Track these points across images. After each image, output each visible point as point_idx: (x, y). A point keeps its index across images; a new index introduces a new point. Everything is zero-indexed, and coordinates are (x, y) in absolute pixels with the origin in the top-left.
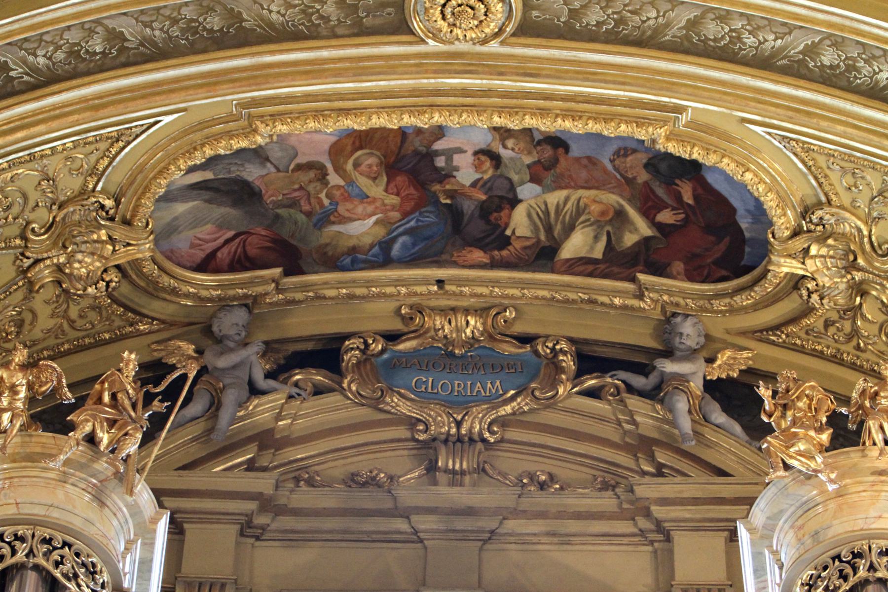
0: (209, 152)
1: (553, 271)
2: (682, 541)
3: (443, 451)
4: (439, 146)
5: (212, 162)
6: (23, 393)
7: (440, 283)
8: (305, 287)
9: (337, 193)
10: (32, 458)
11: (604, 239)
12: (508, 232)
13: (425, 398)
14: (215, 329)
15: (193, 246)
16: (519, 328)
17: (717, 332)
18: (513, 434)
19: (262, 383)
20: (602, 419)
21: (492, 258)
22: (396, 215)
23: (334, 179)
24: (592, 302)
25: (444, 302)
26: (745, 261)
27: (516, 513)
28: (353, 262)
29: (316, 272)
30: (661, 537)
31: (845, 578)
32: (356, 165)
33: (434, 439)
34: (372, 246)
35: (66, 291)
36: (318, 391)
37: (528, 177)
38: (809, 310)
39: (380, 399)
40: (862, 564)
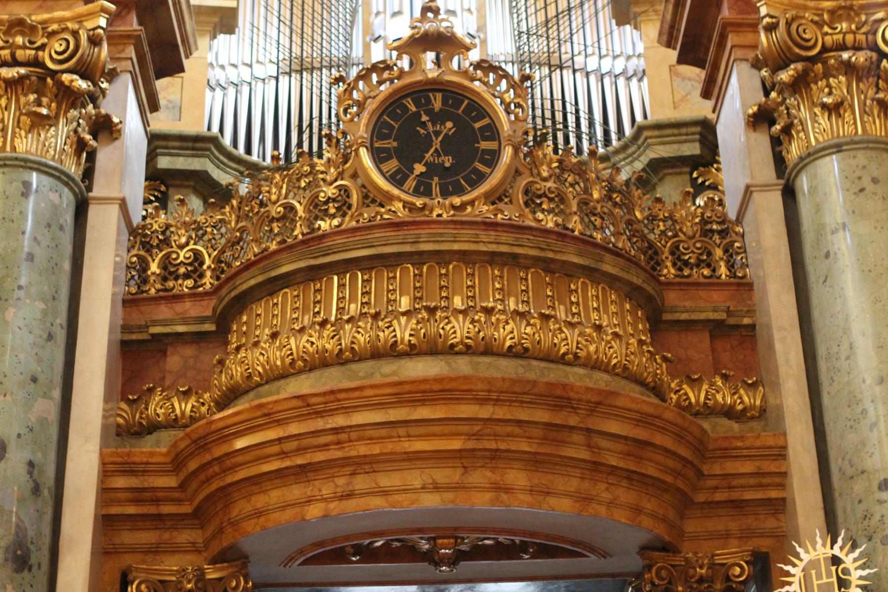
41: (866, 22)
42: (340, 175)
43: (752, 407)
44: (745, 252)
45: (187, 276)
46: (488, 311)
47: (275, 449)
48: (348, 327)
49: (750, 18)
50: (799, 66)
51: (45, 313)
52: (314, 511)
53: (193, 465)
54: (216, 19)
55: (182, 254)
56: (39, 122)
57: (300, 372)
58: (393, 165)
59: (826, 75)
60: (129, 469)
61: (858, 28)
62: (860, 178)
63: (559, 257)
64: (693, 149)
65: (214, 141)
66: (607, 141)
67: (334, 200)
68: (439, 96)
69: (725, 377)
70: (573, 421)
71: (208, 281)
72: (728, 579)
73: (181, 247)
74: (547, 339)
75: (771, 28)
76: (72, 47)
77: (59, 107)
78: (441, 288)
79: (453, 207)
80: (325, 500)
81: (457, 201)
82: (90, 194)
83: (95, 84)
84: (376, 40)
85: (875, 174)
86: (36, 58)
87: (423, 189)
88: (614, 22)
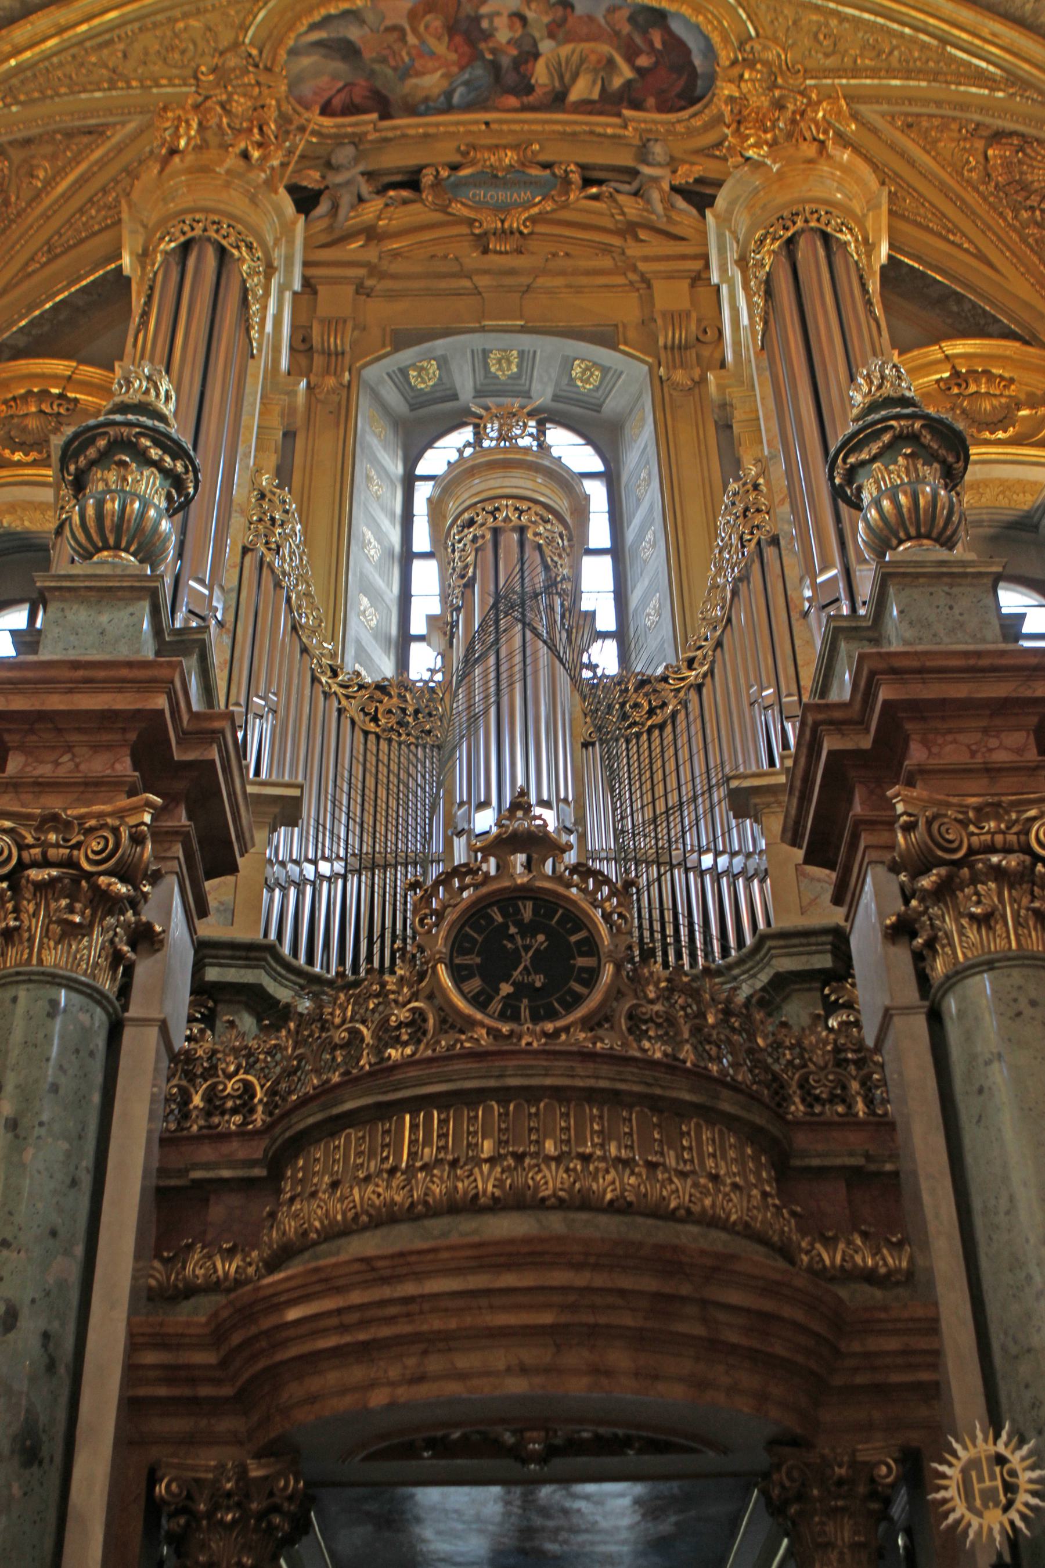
0: (323, 12)
1: (564, 111)
2: (658, 285)
3: (493, 239)
4: (484, 10)
5: (328, 19)
7: (487, 124)
8: (394, 128)
9: (414, 52)
11: (599, 83)
12: (533, 81)
13: (480, 206)
14: (333, 161)
15: (315, 93)
16: (543, 158)
17: (678, 154)
18: (541, 229)
20: (600, 214)
21: (522, 103)
22: (455, 69)
23: (412, 39)
24: (592, 133)
26: (698, 92)
27: (545, 272)
28: (428, 109)
29: (401, 117)
30: (644, 285)
31: (786, 228)
32: (427, 27)
33: (485, 234)
34: (439, 96)
36: (405, 202)
37: (546, 34)
41: (1017, 821)
42: (415, 996)
43: (898, 1270)
44: (886, 1085)
45: (235, 1111)
46: (586, 1158)
47: (334, 1321)
48: (420, 1176)
49: (884, 815)
50: (943, 871)
51: (68, 1155)
52: (378, 1398)
53: (236, 1339)
55: (230, 1086)
56: (71, 931)
57: (365, 1228)
58: (475, 984)
59: (974, 881)
60: (162, 1342)
61: (1008, 828)
62: (1015, 1000)
63: (669, 1093)
64: (825, 961)
65: (272, 950)
66: (725, 951)
67: (407, 1025)
68: (529, 904)
69: (865, 1235)
70: (685, 1290)
71: (259, 1117)
72: (872, 1480)
73: (230, 1077)
74: (654, 1191)
75: (908, 828)
76: (111, 846)
77: (94, 915)
78: (530, 1130)
79: (545, 1034)
80: (392, 1384)
81: (549, 1027)
82: (126, 1015)
83: (136, 888)
84: (459, 834)
85: (1033, 995)
86: (70, 856)
87: (510, 1013)
88: (731, 814)
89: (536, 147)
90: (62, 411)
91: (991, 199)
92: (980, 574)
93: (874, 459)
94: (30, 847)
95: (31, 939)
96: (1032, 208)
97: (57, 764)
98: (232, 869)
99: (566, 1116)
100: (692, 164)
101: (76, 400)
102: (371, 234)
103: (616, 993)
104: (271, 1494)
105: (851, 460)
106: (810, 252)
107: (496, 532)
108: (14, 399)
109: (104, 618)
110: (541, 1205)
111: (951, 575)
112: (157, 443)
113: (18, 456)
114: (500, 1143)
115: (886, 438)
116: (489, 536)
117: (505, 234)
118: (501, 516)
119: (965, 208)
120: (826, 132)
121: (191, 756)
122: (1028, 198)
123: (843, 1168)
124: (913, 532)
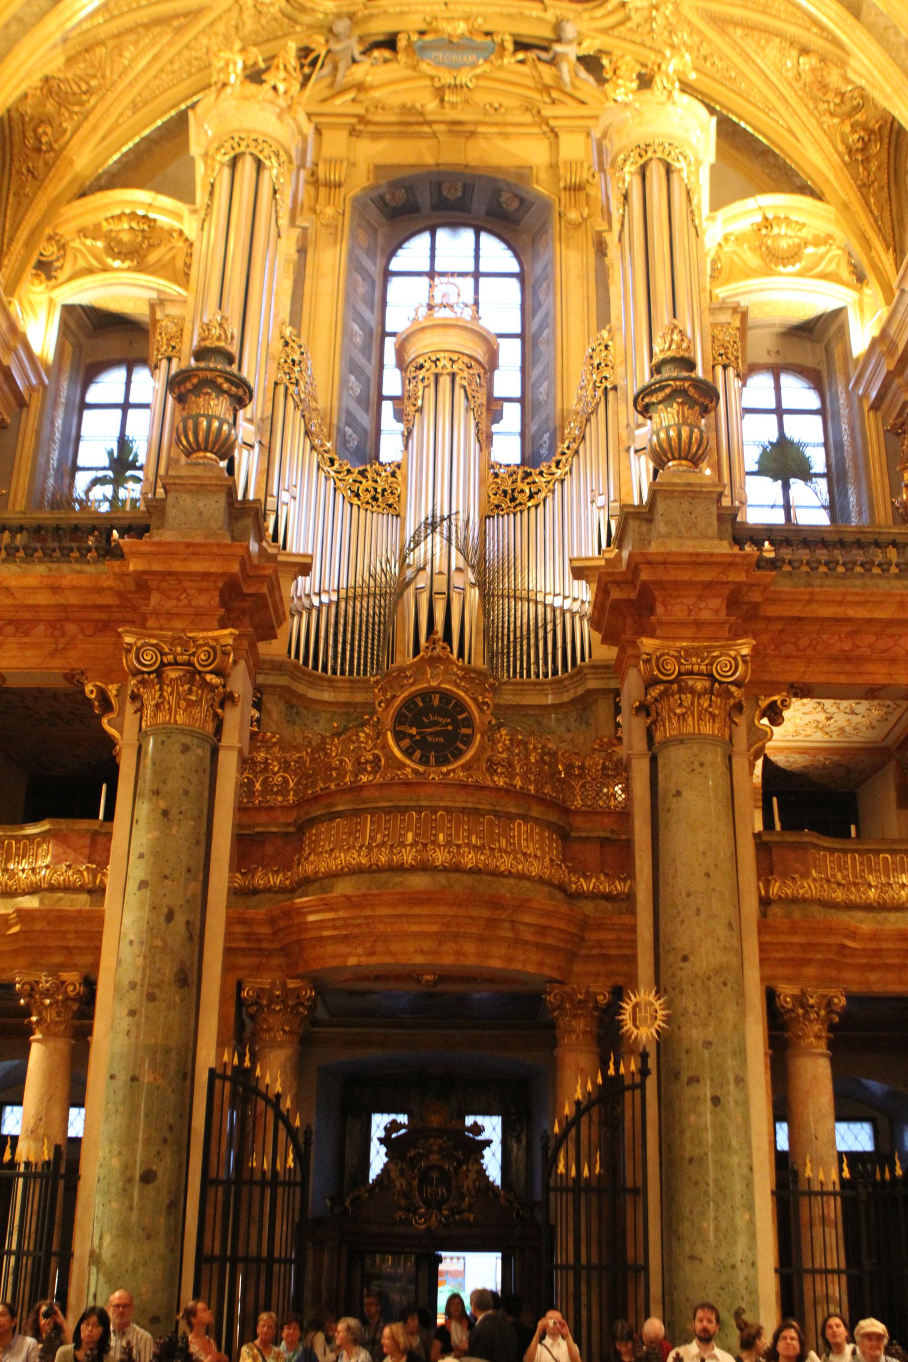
2: (564, 138)
6: (240, 65)
10: (245, 98)
13: (438, 64)
17: (584, 30)
18: (483, 83)
19: (358, 57)
20: (525, 75)
25: (448, 15)
31: (641, 156)
35: (260, 12)
36: (386, 61)
38: (628, 18)
39: (417, 65)
40: (650, 150)
42: (375, 746)
46: (459, 846)
50: (661, 687)
52: (352, 961)
54: (297, 569)
57: (346, 874)
59: (681, 690)
60: (243, 921)
65: (296, 666)
67: (371, 762)
68: (437, 696)
69: (606, 875)
71: (291, 797)
72: (596, 1001)
73: (275, 774)
74: (492, 863)
81: (444, 769)
89: (480, 21)
90: (146, 228)
91: (800, 93)
92: (710, 492)
93: (660, 402)
94: (167, 654)
95: (170, 709)
96: (828, 102)
97: (178, 599)
98: (275, 637)
99: (450, 821)
100: (594, 38)
101: (155, 220)
102: (360, 87)
103: (482, 748)
104: (298, 997)
105: (647, 400)
106: (656, 173)
107: (437, 376)
108: (112, 217)
109: (201, 504)
110: (435, 869)
111: (693, 492)
112: (227, 380)
113: (117, 263)
114: (416, 835)
115: (668, 391)
116: (432, 378)
117: (457, 88)
118: (440, 364)
119: (782, 97)
120: (673, 84)
121: (252, 590)
122: (825, 94)
123: (599, 838)
124: (676, 455)
